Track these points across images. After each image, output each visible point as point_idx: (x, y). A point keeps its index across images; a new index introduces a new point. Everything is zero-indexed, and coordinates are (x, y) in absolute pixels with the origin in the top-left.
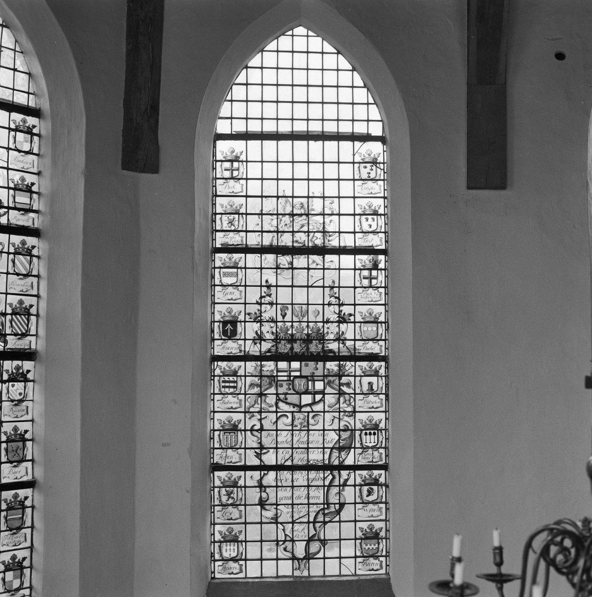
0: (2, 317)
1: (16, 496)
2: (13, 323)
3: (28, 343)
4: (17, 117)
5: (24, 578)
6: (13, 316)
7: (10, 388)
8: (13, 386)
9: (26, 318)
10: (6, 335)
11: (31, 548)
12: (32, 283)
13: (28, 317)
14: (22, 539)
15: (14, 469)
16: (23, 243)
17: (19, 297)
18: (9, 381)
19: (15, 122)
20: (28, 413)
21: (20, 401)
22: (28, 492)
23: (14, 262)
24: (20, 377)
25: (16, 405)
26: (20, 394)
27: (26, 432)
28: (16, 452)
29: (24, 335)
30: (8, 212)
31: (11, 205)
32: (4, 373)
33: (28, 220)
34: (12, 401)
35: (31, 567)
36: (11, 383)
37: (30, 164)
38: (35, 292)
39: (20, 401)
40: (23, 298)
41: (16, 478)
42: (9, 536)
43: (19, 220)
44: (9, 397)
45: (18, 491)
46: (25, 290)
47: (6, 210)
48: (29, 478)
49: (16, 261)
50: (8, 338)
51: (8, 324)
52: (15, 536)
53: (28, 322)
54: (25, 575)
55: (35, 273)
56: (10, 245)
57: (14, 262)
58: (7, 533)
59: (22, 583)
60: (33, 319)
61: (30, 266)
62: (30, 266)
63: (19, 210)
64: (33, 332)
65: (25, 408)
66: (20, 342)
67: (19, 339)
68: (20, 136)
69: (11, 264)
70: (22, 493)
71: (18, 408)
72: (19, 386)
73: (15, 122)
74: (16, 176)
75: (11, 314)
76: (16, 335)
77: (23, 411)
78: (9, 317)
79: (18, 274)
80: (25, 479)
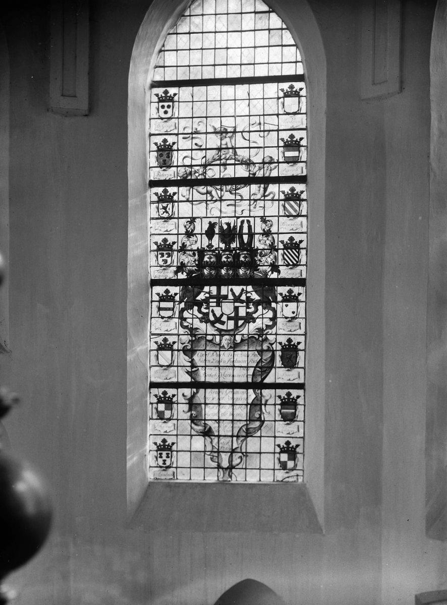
0: (275, 252)
1: (289, 394)
2: (285, 256)
3: (299, 271)
4: (285, 86)
5: (298, 461)
6: (285, 251)
7: (284, 306)
8: (287, 306)
9: (296, 251)
10: (278, 266)
11: (303, 438)
12: (302, 222)
13: (299, 251)
14: (296, 430)
15: (287, 372)
16: (293, 189)
17: (290, 235)
18: (282, 302)
19: (282, 90)
20: (300, 328)
21: (293, 318)
22: (300, 392)
23: (284, 207)
24: (290, 298)
25: (289, 321)
26: (293, 313)
27: (299, 343)
28: (290, 358)
29: (295, 265)
30: (278, 165)
31: (281, 160)
32: (278, 295)
33: (297, 170)
34: (286, 318)
35: (303, 453)
36: (284, 304)
37: (299, 122)
38: (304, 230)
39: (293, 318)
40: (293, 235)
41: (289, 380)
42: (283, 425)
43: (288, 171)
44: (283, 315)
45: (291, 391)
46: (295, 229)
47: (277, 164)
48: (301, 381)
49: (287, 205)
50: (281, 268)
51: (280, 258)
52: (289, 426)
53: (299, 255)
54: (298, 459)
55: (304, 213)
56: (280, 193)
57: (284, 207)
58: (281, 423)
59: (296, 465)
60: (303, 252)
61: (299, 208)
62: (299, 208)
63: (288, 163)
64: (303, 261)
65: (298, 324)
66: (292, 271)
67: (291, 269)
68: (288, 100)
69: (281, 208)
70: (295, 393)
71: (291, 324)
72: (292, 306)
73: (282, 90)
74: (285, 135)
75: (283, 249)
76: (288, 265)
77: (297, 326)
78: (281, 252)
79: (288, 216)
80: (296, 381)
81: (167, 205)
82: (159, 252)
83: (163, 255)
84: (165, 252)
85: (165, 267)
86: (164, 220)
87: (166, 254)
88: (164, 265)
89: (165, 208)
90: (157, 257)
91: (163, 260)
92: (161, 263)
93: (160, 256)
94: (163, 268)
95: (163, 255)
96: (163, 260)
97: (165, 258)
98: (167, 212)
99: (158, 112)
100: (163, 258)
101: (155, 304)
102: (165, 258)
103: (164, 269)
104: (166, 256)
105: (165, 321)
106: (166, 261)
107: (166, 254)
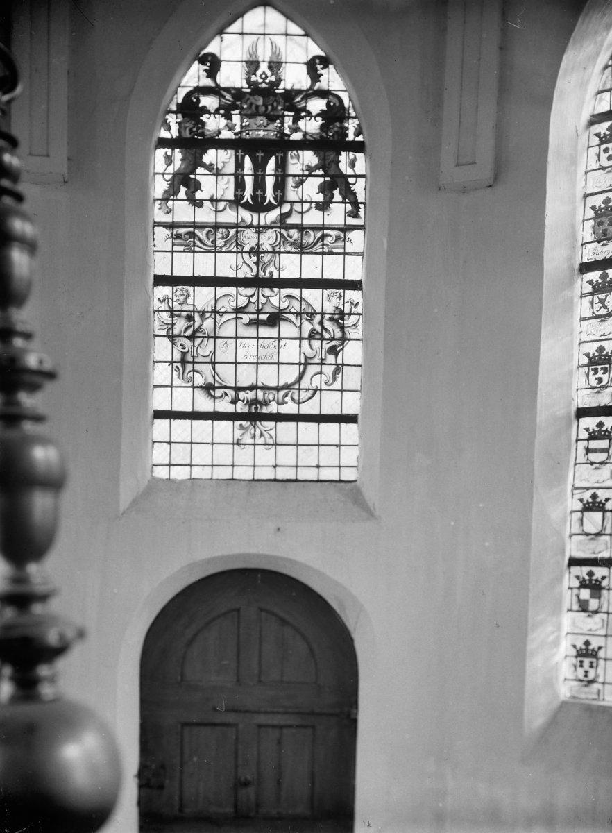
81: (606, 296)
82: (591, 368)
83: (596, 371)
84: (599, 367)
85: (599, 389)
86: (600, 319)
87: (602, 369)
88: (598, 386)
89: (602, 301)
90: (588, 375)
91: (596, 379)
92: (594, 383)
93: (593, 372)
94: (596, 390)
95: (596, 371)
96: (596, 379)
97: (599, 375)
98: (605, 307)
99: (599, 161)
100: (597, 376)
101: (582, 445)
102: (599, 375)
103: (598, 392)
104: (600, 372)
105: (596, 468)
106: (600, 380)
107: (602, 369)
